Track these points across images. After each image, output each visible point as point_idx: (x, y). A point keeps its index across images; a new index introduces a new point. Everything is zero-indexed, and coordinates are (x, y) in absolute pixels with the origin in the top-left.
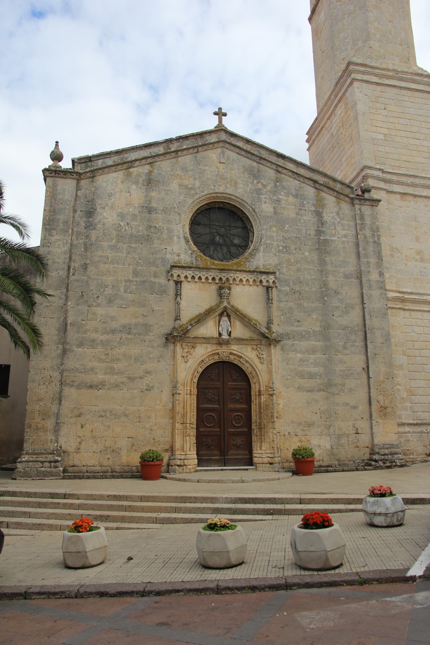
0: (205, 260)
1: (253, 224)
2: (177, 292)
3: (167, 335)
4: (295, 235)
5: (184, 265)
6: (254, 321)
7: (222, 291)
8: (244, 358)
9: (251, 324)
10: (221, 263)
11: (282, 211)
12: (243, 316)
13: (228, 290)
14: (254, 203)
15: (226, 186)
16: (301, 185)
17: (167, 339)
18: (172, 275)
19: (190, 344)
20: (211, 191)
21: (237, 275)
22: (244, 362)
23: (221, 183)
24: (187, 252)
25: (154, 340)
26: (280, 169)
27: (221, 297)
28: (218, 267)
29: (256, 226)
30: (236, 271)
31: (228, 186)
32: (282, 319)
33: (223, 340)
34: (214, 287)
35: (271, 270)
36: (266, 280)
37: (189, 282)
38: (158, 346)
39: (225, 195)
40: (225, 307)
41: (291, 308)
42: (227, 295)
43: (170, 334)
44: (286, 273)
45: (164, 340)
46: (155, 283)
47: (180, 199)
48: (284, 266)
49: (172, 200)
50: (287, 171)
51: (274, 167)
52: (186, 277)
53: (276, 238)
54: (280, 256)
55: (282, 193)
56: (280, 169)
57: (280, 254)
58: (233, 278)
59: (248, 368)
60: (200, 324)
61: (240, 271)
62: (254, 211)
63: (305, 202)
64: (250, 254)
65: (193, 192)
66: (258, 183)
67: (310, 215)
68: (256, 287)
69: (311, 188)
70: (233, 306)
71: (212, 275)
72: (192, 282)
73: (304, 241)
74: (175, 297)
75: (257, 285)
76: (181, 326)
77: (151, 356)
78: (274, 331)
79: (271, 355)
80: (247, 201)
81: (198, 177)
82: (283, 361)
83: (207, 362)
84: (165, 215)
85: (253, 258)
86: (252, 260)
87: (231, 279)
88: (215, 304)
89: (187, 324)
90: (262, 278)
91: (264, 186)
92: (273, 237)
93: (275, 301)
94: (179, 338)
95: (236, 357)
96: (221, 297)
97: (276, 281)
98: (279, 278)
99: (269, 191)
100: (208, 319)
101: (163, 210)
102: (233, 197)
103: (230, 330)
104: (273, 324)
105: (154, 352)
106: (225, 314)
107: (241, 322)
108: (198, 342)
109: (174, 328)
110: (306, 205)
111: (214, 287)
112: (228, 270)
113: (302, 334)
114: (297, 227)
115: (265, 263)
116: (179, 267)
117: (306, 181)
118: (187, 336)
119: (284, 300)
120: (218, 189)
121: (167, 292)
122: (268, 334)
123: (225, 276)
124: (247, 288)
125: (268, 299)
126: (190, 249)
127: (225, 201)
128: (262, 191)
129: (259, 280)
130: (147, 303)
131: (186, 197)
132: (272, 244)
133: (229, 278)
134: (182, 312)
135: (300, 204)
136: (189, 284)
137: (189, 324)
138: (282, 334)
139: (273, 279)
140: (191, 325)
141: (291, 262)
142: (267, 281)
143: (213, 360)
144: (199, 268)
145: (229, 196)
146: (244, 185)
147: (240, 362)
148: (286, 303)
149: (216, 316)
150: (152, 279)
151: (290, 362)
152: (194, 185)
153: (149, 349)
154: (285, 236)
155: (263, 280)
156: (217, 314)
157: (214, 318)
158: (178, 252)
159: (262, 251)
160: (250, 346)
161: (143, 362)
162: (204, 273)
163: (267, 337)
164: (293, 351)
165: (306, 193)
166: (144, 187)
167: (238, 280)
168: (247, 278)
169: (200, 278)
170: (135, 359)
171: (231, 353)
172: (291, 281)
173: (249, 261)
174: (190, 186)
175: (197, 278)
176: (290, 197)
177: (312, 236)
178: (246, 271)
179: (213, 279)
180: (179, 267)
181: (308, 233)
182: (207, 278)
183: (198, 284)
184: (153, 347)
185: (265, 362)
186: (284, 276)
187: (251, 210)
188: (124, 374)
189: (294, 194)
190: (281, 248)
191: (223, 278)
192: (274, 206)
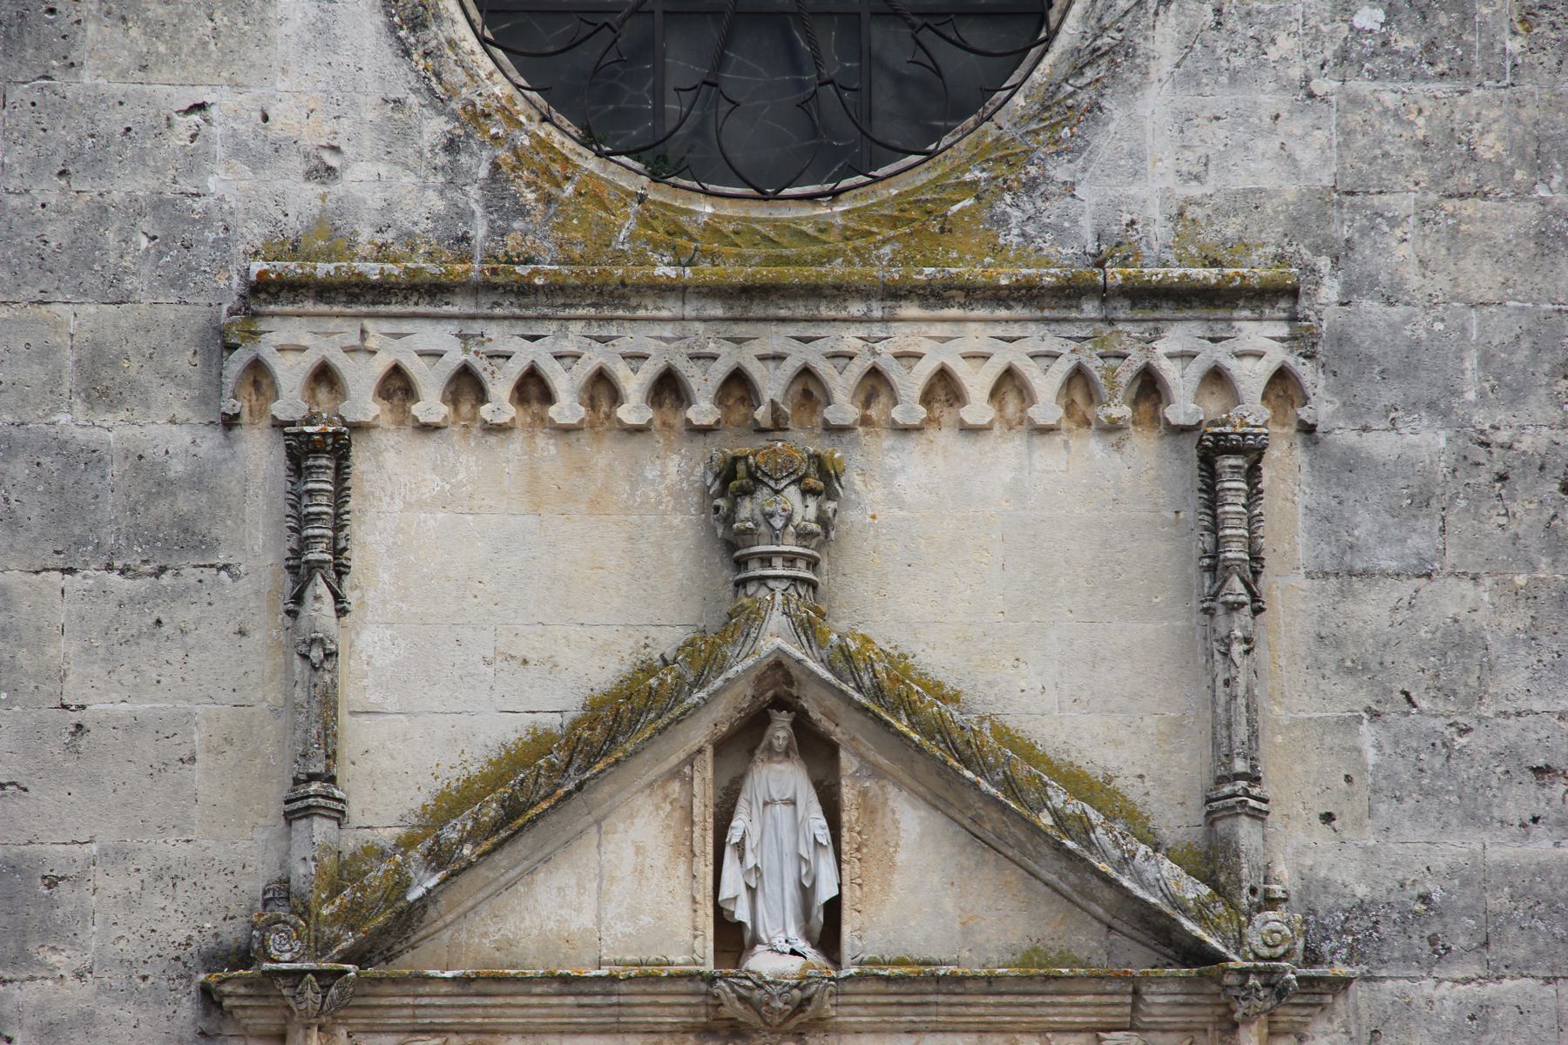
0: (593, 194)
2: (305, 544)
5: (373, 271)
6: (1058, 797)
7: (746, 508)
9: (1036, 830)
10: (759, 211)
12: (953, 748)
13: (807, 492)
17: (209, 998)
18: (258, 371)
21: (903, 337)
24: (405, 134)
27: (741, 564)
28: (707, 271)
30: (894, 293)
32: (1371, 756)
33: (756, 994)
34: (674, 464)
35: (1257, 270)
36: (1196, 369)
37: (427, 429)
40: (779, 667)
42: (790, 546)
43: (243, 956)
44: (1414, 280)
45: (188, 1009)
46: (93, 457)
48: (1403, 203)
52: (397, 385)
54: (1355, 101)
57: (1362, 86)
58: (857, 369)
60: (527, 841)
61: (935, 295)
64: (1048, 102)
68: (1093, 447)
70: (848, 657)
71: (650, 347)
72: (455, 431)
74: (287, 583)
75: (1112, 428)
76: (344, 873)
78: (1285, 877)
85: (1075, 152)
86: (1060, 171)
87: (842, 385)
88: (679, 635)
89: (407, 844)
90: (1161, 347)
93: (1301, 581)
94: (311, 995)
96: (741, 564)
97: (1306, 372)
98: (1341, 339)
100: (606, 789)
103: (826, 892)
104: (1258, 816)
106: (780, 731)
107: (935, 802)
108: (516, 1018)
109: (281, 892)
111: (674, 464)
112: (814, 292)
115: (1195, 190)
116: (325, 291)
118: (404, 965)
119: (1386, 560)
121: (210, 545)
122: (1200, 919)
123: (779, 358)
125: (1215, 566)
126: (438, 103)
129: (1126, 373)
130: (23, 656)
133: (824, 368)
134: (355, 734)
136: (429, 447)
137: (416, 854)
138: (1362, 907)
139: (1278, 355)
140: (438, 857)
141: (1472, 156)
142: (1217, 377)
144: (523, 290)
148: (1406, 588)
149: (690, 760)
150: (72, 421)
155: (1170, 372)
156: (699, 733)
157: (675, 773)
158: (312, 135)
159: (1163, 66)
162: (573, 337)
163: (1196, 955)
167: (911, 382)
168: (1004, 356)
169: (533, 388)
172: (1471, 362)
173: (1031, 185)
175: (500, 388)
178: (997, 296)
179: (668, 388)
180: (325, 291)
182: (602, 386)
183: (516, 444)
186: (1397, 312)
191: (756, 371)
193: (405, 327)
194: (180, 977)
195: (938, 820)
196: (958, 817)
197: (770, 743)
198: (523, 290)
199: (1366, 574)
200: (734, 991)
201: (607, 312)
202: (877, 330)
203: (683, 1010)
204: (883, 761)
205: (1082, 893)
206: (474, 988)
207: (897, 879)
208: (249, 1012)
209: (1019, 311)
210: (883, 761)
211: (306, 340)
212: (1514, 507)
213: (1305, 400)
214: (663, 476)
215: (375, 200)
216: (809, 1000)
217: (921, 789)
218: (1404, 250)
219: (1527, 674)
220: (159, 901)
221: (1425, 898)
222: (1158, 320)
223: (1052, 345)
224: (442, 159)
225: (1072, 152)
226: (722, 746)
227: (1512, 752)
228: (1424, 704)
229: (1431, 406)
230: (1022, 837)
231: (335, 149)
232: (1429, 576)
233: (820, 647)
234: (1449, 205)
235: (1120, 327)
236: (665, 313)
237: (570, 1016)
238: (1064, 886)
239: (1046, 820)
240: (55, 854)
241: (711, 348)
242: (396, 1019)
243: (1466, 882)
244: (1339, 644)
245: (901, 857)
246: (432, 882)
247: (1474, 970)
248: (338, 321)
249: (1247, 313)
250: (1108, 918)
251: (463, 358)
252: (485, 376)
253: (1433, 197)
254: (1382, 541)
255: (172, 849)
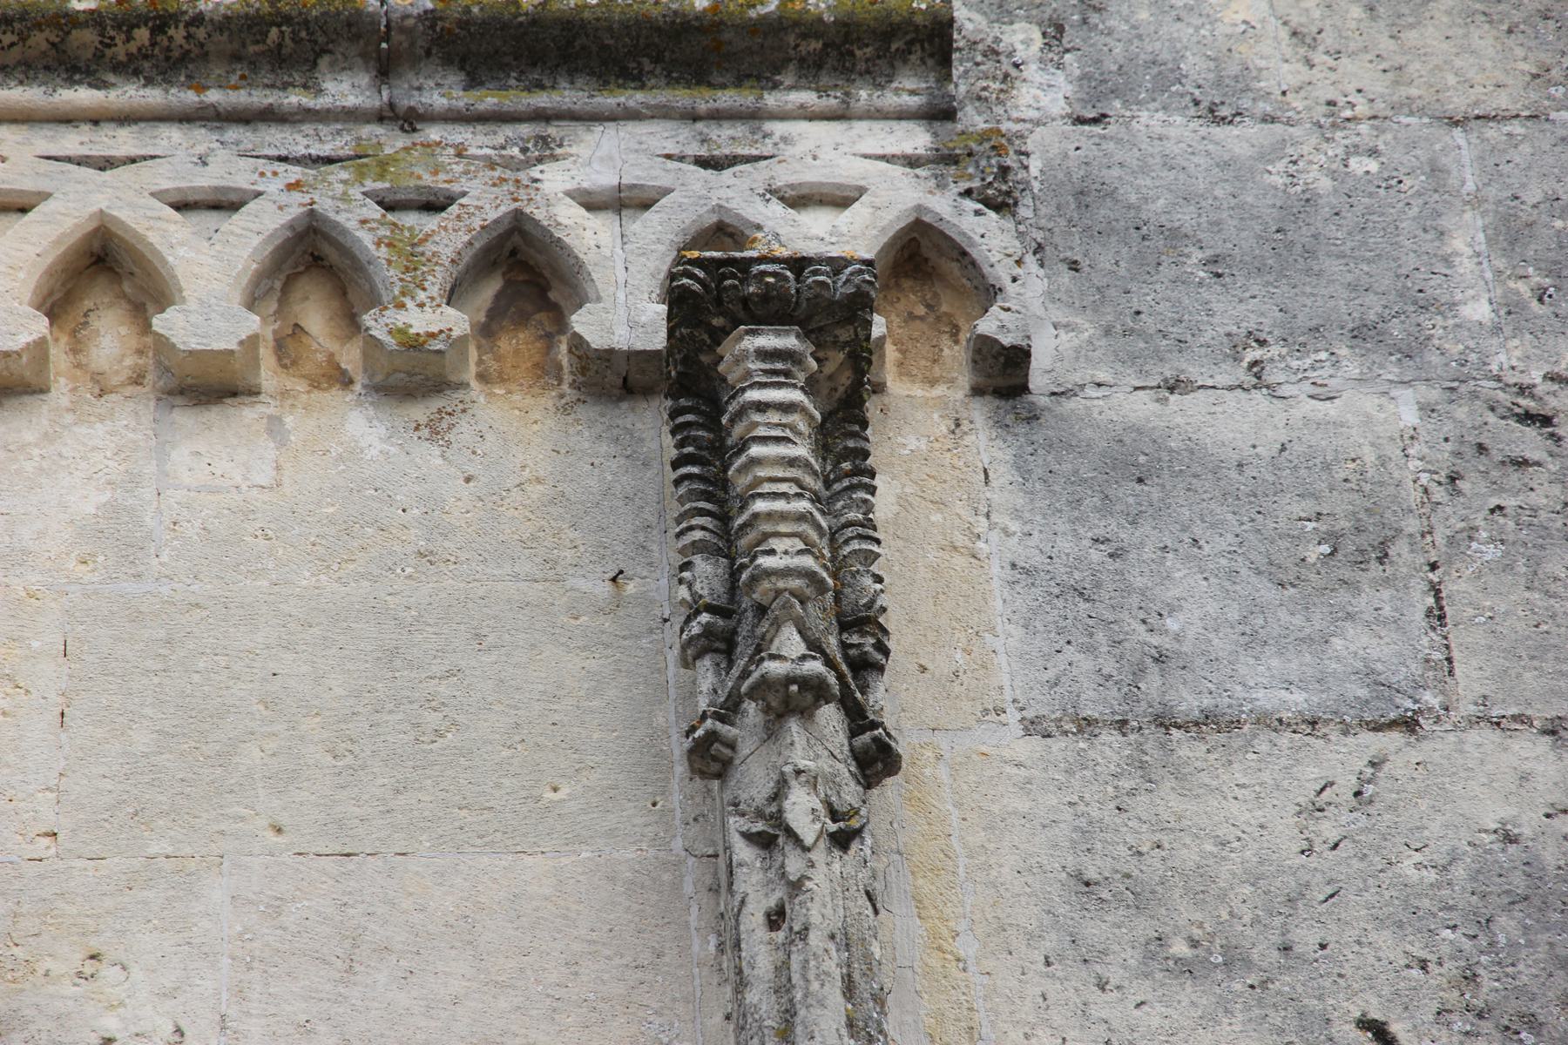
90: (555, 179)
186: (1240, 139)
199: (1207, 721)
209: (129, 94)
213: (988, 293)
229: (1360, 334)
232: (1409, 724)
235: (434, 133)
244: (1140, 898)
249: (807, 97)
254: (1253, 641)
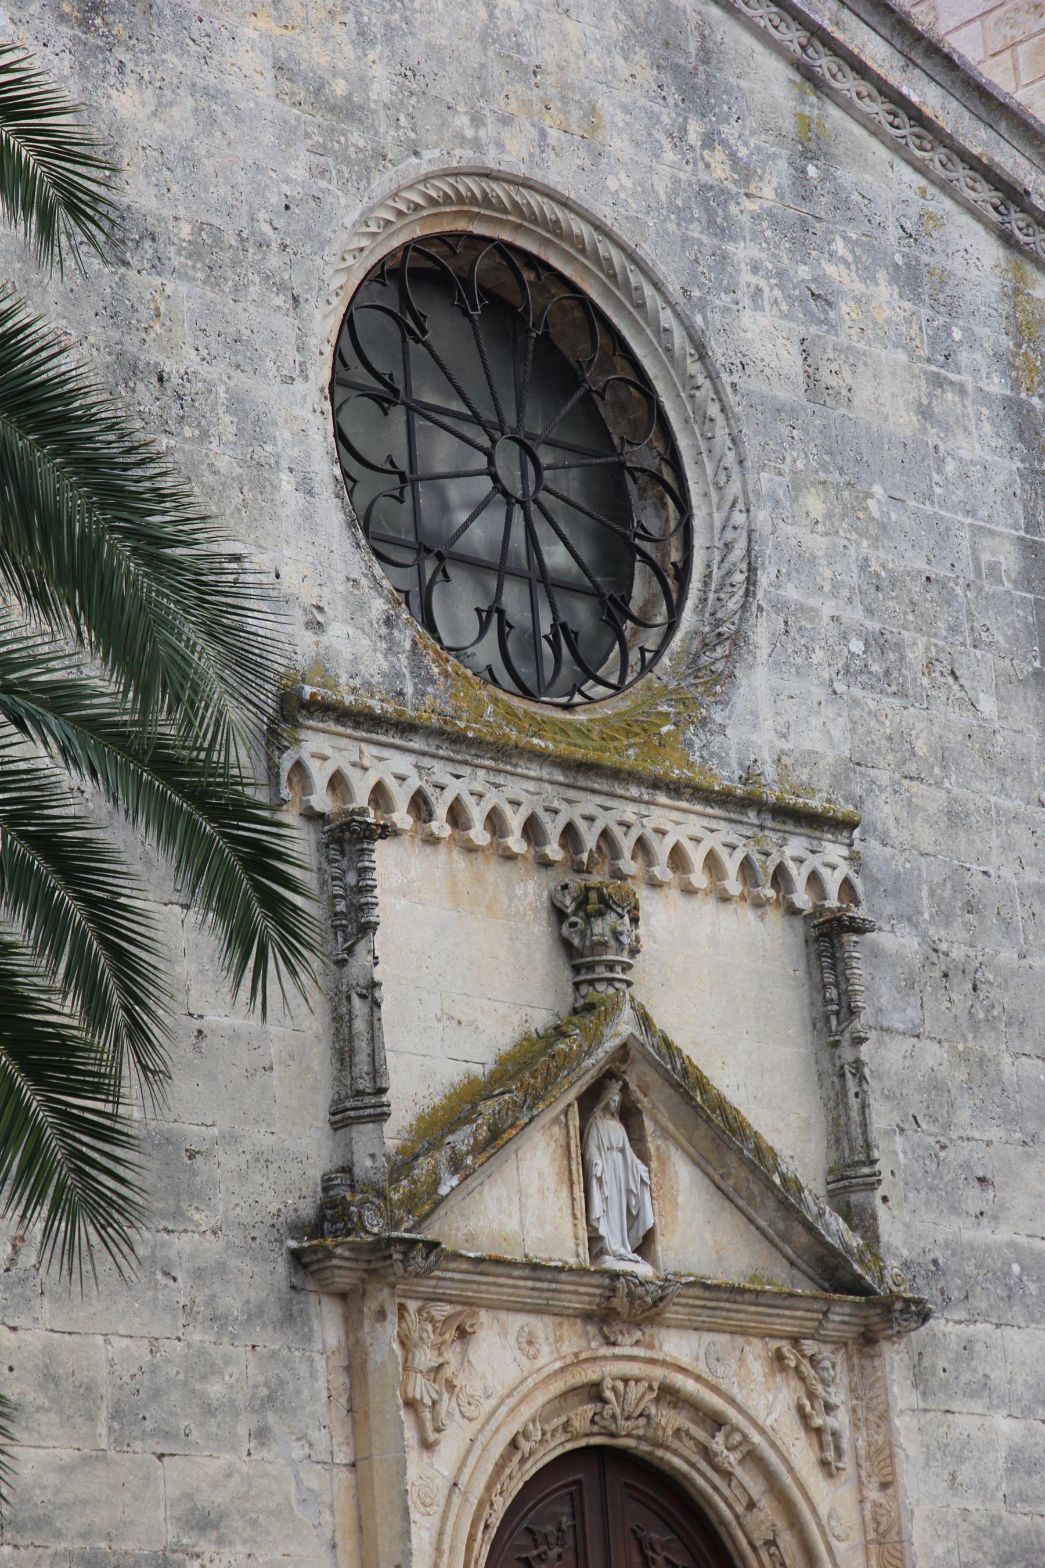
1: (683, 443)
3: (296, 1229)
4: (920, 564)
8: (736, 1429)
11: (846, 373)
14: (696, 293)
15: (543, 134)
16: (931, 206)
19: (448, 1309)
20: (463, 157)
21: (658, 817)
22: (731, 1459)
23: (513, 106)
24: (361, 606)
25: (221, 1268)
26: (824, 63)
28: (563, 749)
29: (709, 468)
31: (553, 134)
36: (805, 870)
38: (254, 1315)
39: (534, 200)
41: (936, 1086)
45: (281, 1267)
47: (287, 181)
49: (240, 177)
50: (865, 87)
51: (792, 36)
53: (828, 574)
54: (856, 702)
55: (840, 247)
56: (824, 63)
59: (751, 1505)
62: (702, 354)
63: (957, 334)
65: (357, 138)
66: (709, 140)
67: (987, 427)
68: (750, 915)
69: (979, 228)
71: (523, 797)
73: (970, 613)
77: (215, 1390)
79: (885, 1417)
80: (662, 269)
81: (378, 29)
82: (927, 1464)
83: (531, 1453)
84: (210, 295)
91: (744, 172)
92: (813, 561)
95: (688, 1425)
99: (771, 214)
101: (195, 251)
102: (579, 227)
105: (227, 1360)
108: (492, 1294)
110: (964, 356)
111: (531, 886)
112: (616, 774)
113: (1007, 1274)
114: (928, 508)
115: (785, 746)
117: (961, 174)
120: (500, 146)
122: (861, 1262)
124: (706, 909)
127: (521, 242)
128: (734, 209)
131: (323, 172)
132: (812, 614)
135: (934, 341)
139: (844, 869)
143: (561, 1437)
144: (456, 739)
145: (560, 213)
146: (637, 144)
147: (706, 1453)
151: (966, 1473)
152: (363, 81)
153: (197, 1336)
154: (874, 566)
157: (555, 1120)
158: (309, 595)
160: (757, 1344)
161: (166, 1435)
164: (972, 1394)
165: (956, 265)
166: (63, 29)
170: (116, 1415)
171: (668, 1394)
172: (925, 893)
174: (340, 87)
176: (882, 276)
177: (1008, 585)
181: (985, 557)
183: (440, 856)
184: (218, 1320)
185: (847, 1462)
187: (679, 338)
188: (59, 1535)
189: (898, 258)
190: (857, 646)
192: (801, 330)
193: (386, 753)
194: (276, 1240)
195: (699, 1174)
196: (712, 1173)
197: (607, 1106)
198: (456, 739)
200: (628, 1286)
201: (501, 766)
202: (643, 809)
203: (587, 1299)
204: (671, 1127)
205: (782, 1238)
206: (482, 1267)
207: (680, 1214)
208: (342, 1272)
209: (717, 811)
210: (671, 1127)
211: (328, 752)
212: (954, 996)
214: (526, 895)
215: (347, 653)
216: (661, 1299)
217: (692, 1150)
218: (887, 809)
219: (969, 1112)
220: (259, 1179)
221: (935, 1262)
222: (785, 832)
223: (733, 839)
224: (384, 631)
225: (724, 702)
226: (580, 1099)
227: (965, 1166)
228: (924, 1126)
229: (909, 919)
230: (756, 1192)
231: (320, 609)
232: (918, 1036)
233: (653, 1036)
234: (906, 782)
235: (767, 832)
236: (532, 773)
237: (524, 1296)
238: (770, 1232)
239: (777, 1180)
240: (193, 1133)
241: (556, 804)
242: (425, 1286)
243: (954, 1253)
245: (681, 1199)
246: (454, 1181)
247: (963, 1315)
248: (346, 740)
249: (829, 836)
250: (793, 1257)
251: (420, 783)
252: (433, 799)
253: (897, 776)
254: (895, 1008)
255: (260, 1137)
